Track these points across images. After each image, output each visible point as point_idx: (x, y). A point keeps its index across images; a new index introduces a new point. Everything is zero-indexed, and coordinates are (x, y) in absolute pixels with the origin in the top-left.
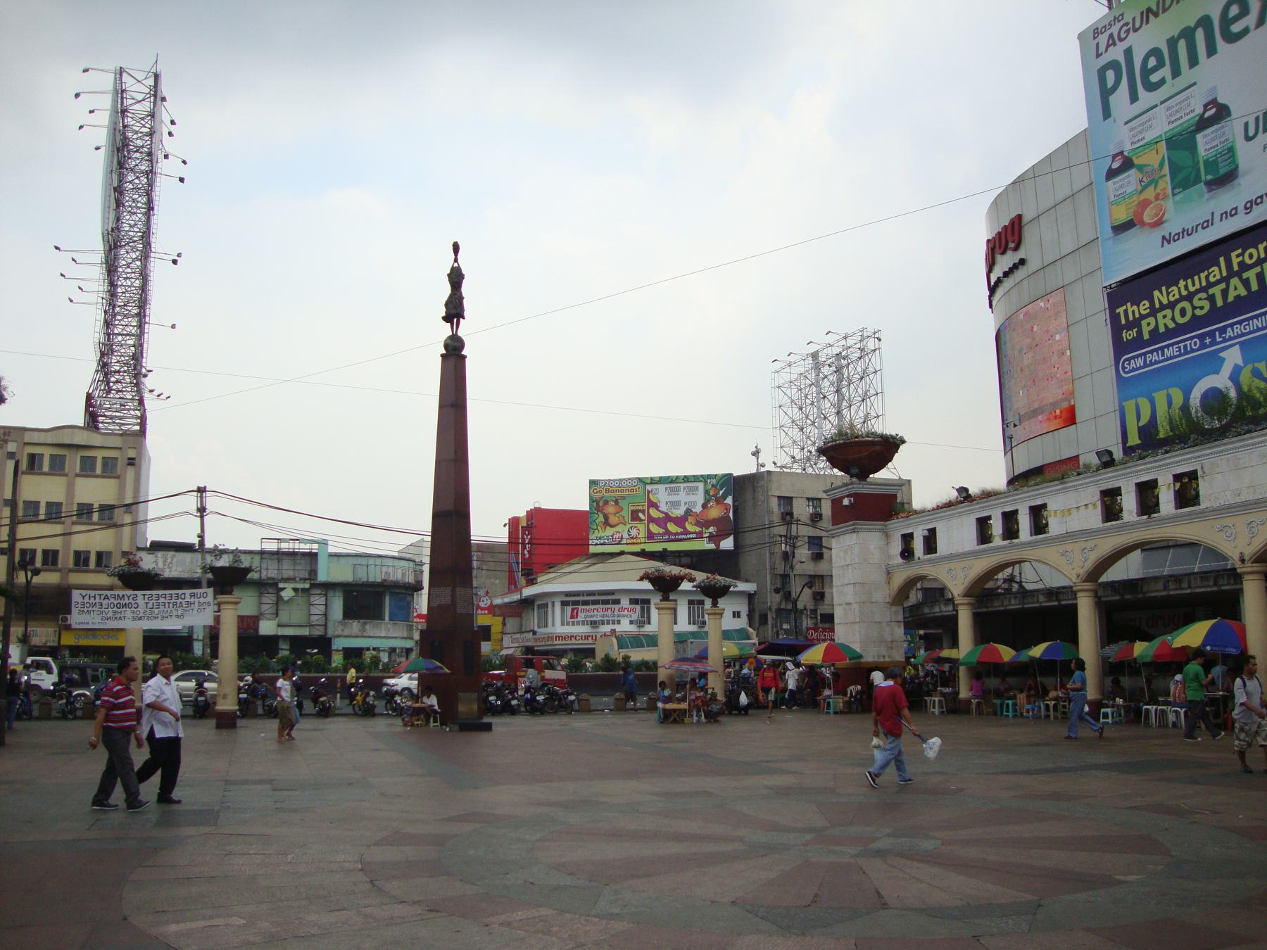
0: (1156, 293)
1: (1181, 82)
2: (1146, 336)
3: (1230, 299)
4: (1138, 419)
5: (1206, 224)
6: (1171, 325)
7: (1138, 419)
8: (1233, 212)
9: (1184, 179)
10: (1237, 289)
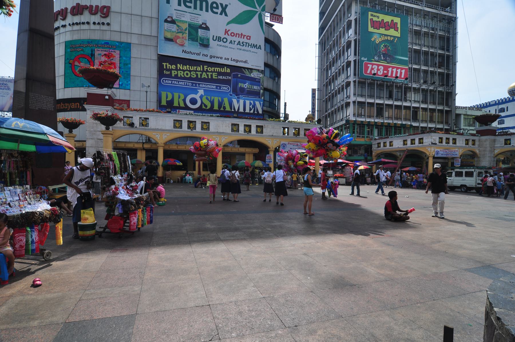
0: (178, 65)
1: (195, 11)
2: (173, 75)
3: (203, 77)
4: (167, 98)
5: (198, 54)
6: (183, 76)
7: (167, 98)
8: (207, 56)
9: (193, 37)
10: (204, 75)
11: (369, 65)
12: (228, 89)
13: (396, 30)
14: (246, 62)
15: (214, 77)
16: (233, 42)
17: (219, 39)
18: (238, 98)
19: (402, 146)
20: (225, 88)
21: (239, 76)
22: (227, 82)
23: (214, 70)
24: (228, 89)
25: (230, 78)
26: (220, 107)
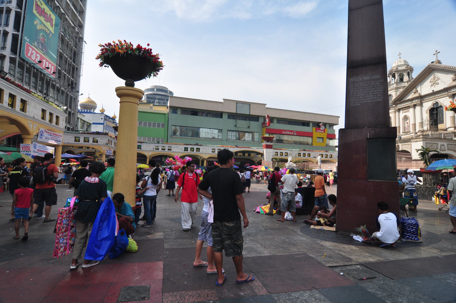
11: (30, 48)
13: (52, 25)
19: (74, 142)
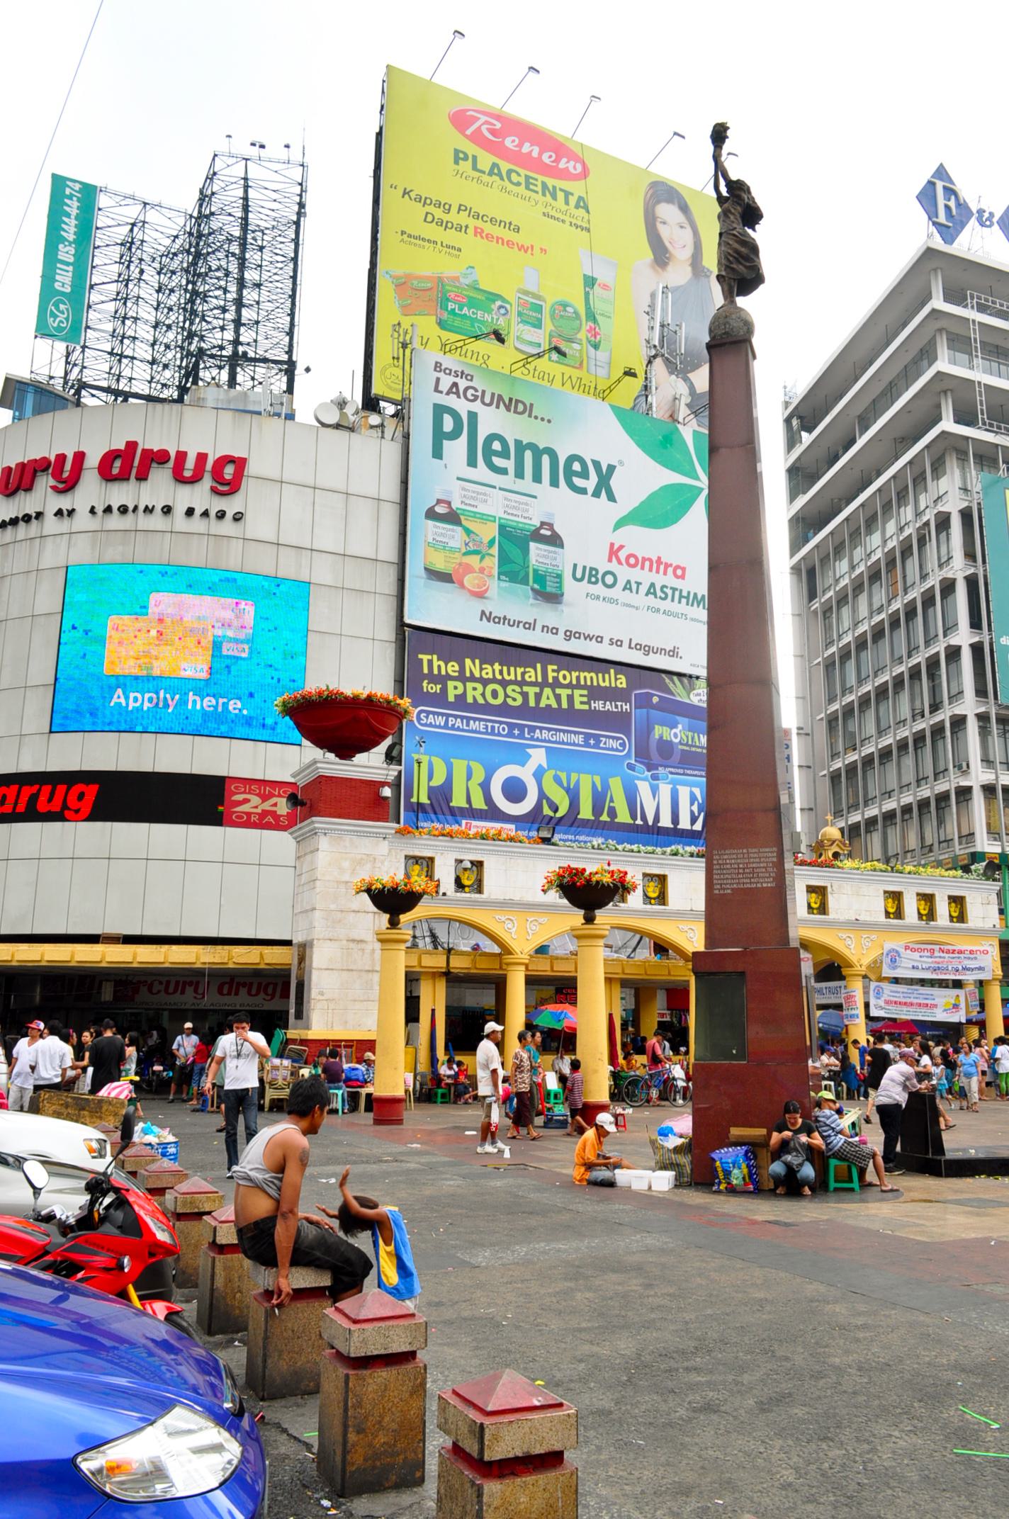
0: (468, 662)
2: (451, 699)
3: (542, 705)
4: (430, 778)
5: (529, 626)
6: (481, 701)
7: (430, 778)
8: (555, 631)
9: (513, 571)
10: (548, 699)
12: (623, 745)
14: (673, 653)
15: (578, 706)
16: (634, 587)
17: (591, 576)
18: (655, 777)
20: (612, 743)
21: (655, 700)
22: (618, 722)
23: (578, 678)
24: (623, 745)
25: (626, 707)
26: (597, 810)
